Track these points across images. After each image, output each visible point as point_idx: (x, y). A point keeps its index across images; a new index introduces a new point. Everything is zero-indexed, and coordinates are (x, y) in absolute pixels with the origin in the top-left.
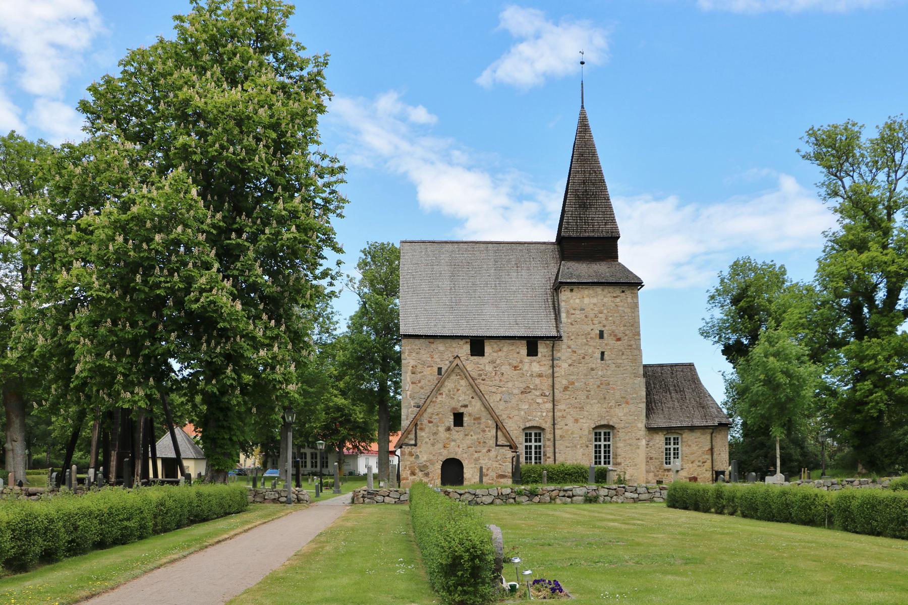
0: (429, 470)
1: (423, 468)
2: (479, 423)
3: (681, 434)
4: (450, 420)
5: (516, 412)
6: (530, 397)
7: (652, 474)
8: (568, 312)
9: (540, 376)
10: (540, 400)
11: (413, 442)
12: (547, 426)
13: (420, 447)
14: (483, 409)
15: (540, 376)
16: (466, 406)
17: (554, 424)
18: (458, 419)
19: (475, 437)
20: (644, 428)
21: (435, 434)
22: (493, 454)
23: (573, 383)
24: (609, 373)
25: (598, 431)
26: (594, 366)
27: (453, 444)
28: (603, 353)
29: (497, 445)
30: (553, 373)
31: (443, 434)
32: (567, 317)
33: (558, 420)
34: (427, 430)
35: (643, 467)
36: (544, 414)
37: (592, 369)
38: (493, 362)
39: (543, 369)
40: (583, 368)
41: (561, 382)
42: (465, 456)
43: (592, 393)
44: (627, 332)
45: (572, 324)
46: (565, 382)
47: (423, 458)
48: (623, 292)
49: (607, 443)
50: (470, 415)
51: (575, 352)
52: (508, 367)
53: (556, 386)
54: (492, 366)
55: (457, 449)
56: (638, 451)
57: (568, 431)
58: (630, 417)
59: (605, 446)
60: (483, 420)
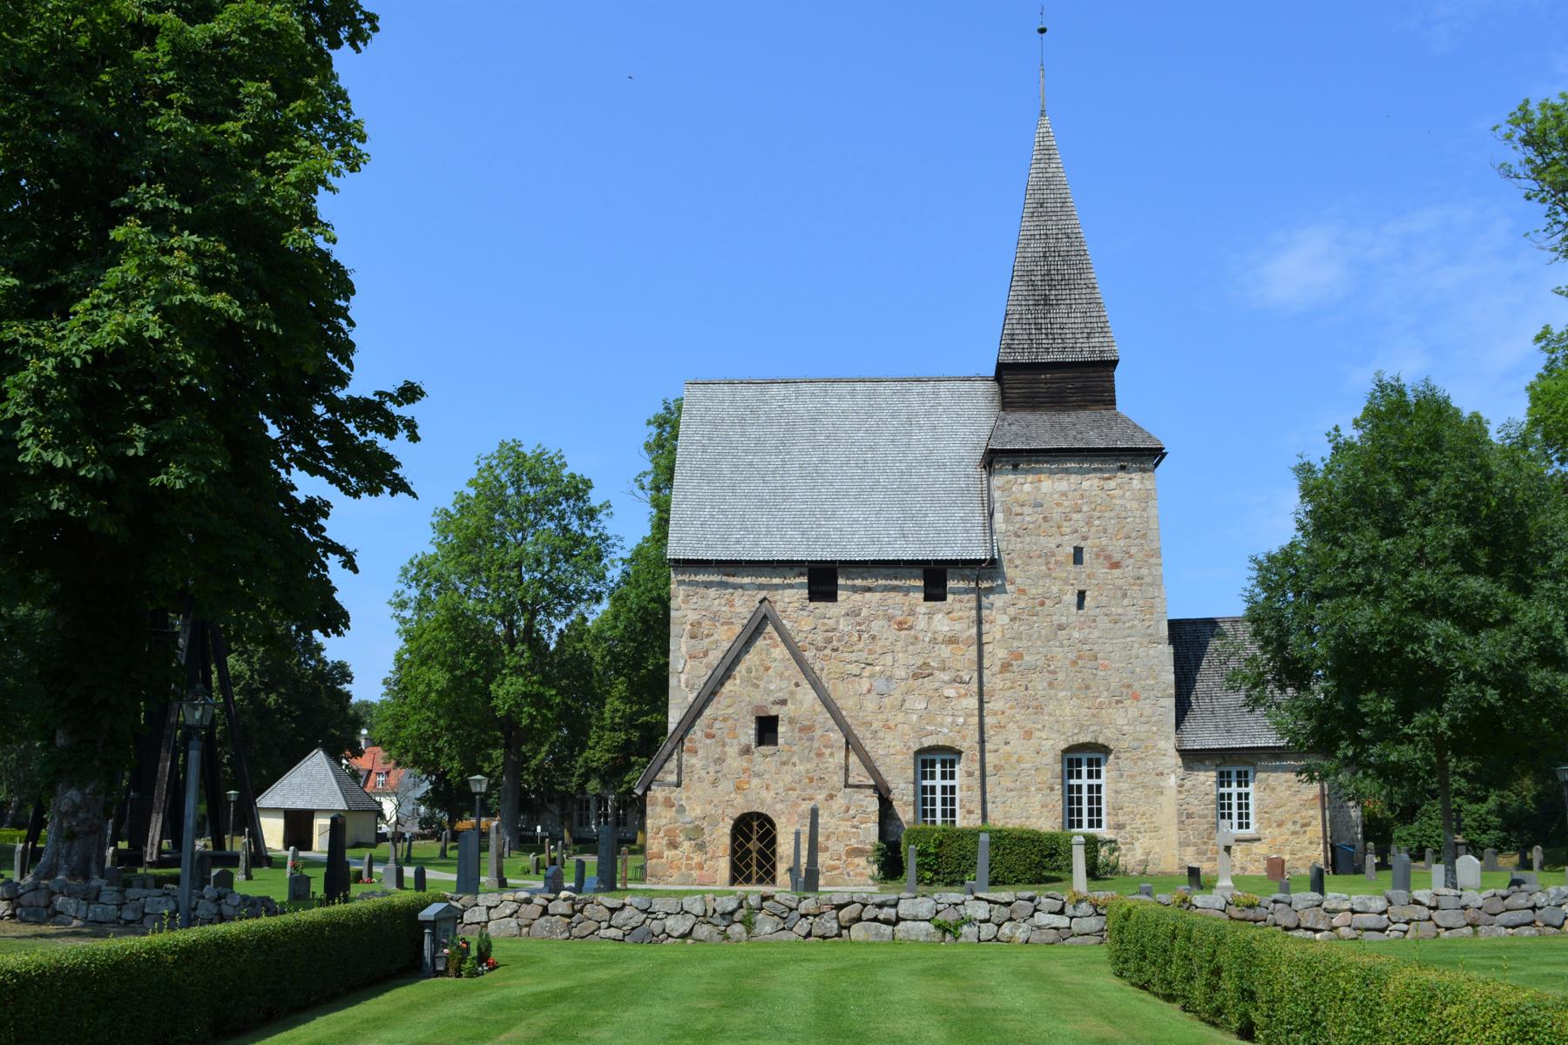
0: (706, 837)
1: (695, 834)
2: (812, 739)
4: (749, 733)
5: (900, 717)
7: (1191, 850)
8: (1008, 512)
9: (952, 641)
10: (950, 692)
12: (968, 744)
13: (687, 787)
14: (819, 707)
15: (952, 641)
16: (783, 702)
17: (982, 742)
18: (767, 729)
20: (1173, 752)
21: (720, 760)
22: (840, 802)
23: (1021, 656)
24: (1096, 634)
25: (1075, 756)
26: (1064, 620)
27: (755, 781)
28: (1081, 595)
30: (980, 634)
31: (735, 762)
32: (1007, 521)
33: (989, 732)
34: (701, 753)
35: (1172, 834)
36: (961, 720)
37: (1061, 627)
38: (853, 613)
39: (957, 627)
41: (996, 654)
42: (778, 807)
43: (1061, 676)
44: (1133, 550)
46: (1001, 653)
47: (695, 811)
48: (1123, 468)
49: (1094, 782)
50: (791, 721)
51: (1023, 592)
53: (986, 663)
54: (852, 620)
55: (764, 793)
56: (1160, 799)
57: (1009, 755)
58: (1142, 723)
59: (1090, 787)
60: (818, 733)
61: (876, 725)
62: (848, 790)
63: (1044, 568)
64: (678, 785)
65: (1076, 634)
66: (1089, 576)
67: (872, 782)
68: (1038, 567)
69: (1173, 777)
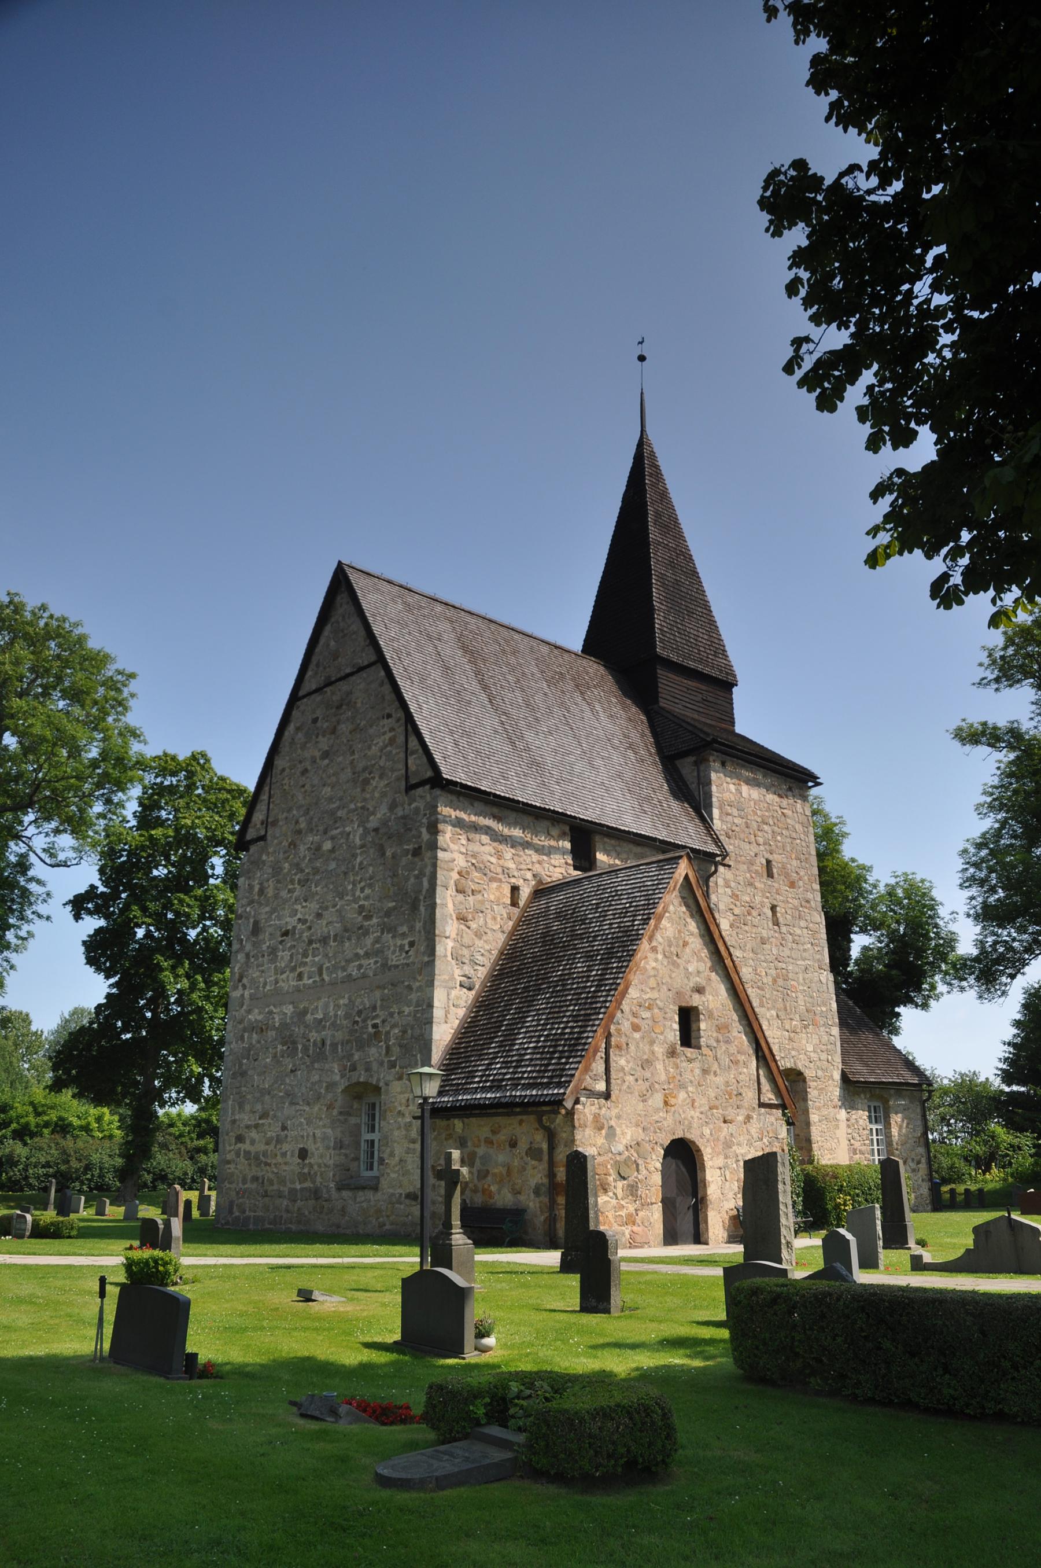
11: (601, 1086)
22: (754, 1128)
29: (762, 1105)
31: (661, 1069)
56: (837, 1131)
62: (763, 1110)
64: (607, 1095)
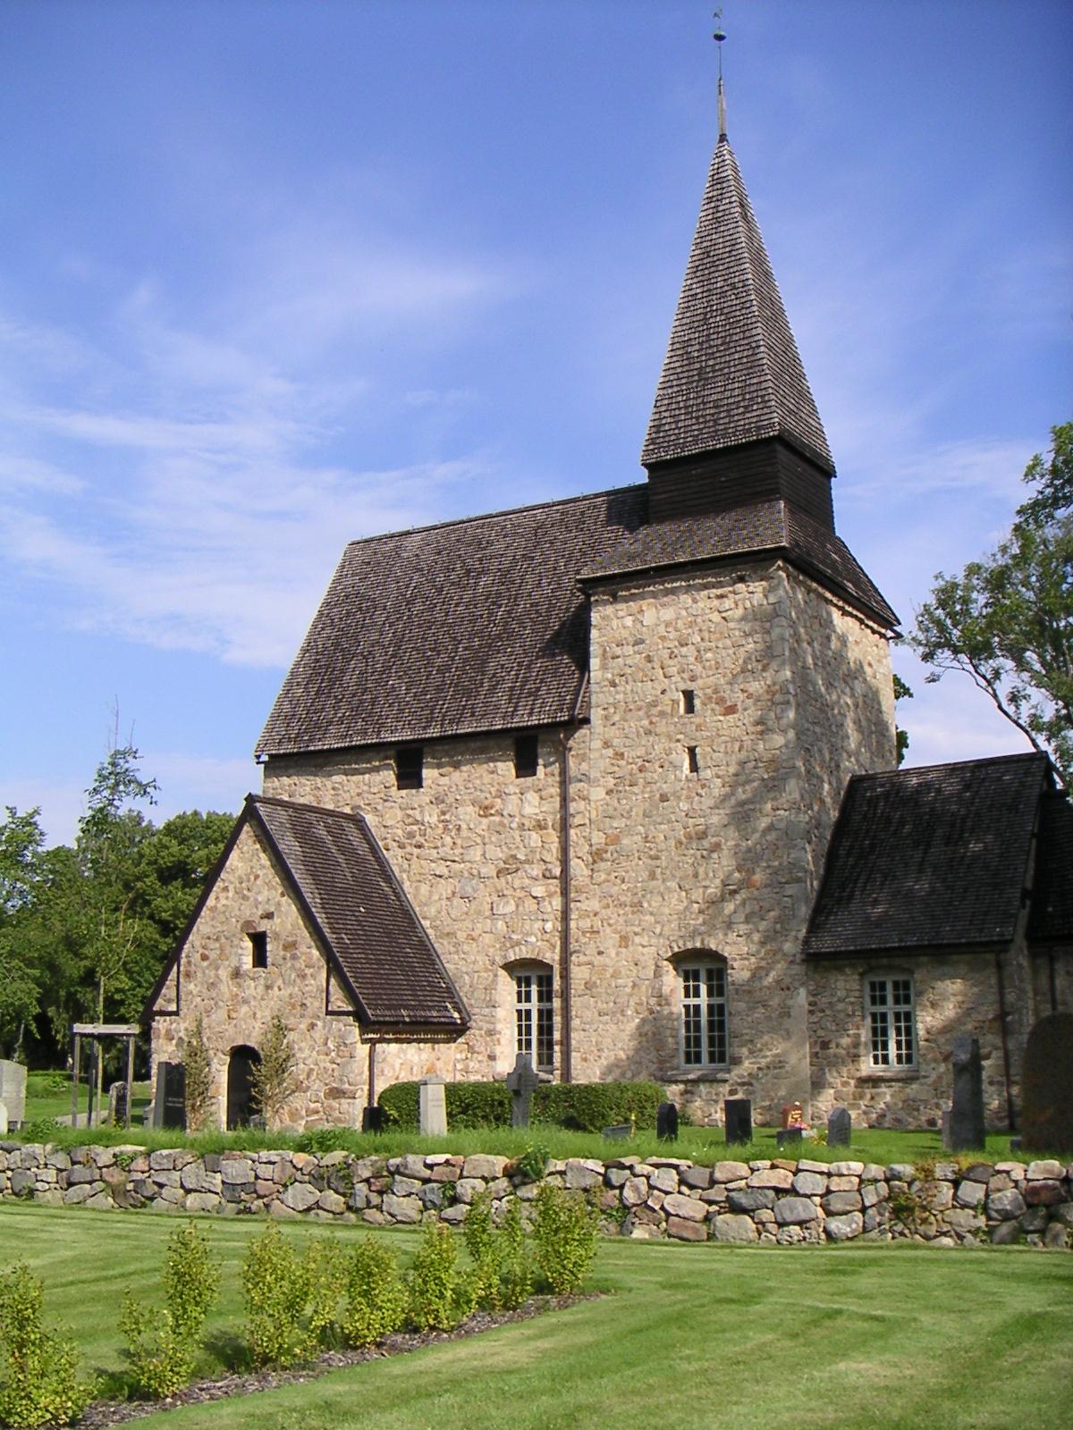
2: (294, 957)
3: (911, 972)
6: (517, 884)
15: (540, 826)
16: (269, 916)
19: (285, 993)
23: (615, 840)
27: (244, 1009)
29: (328, 1013)
32: (604, 667)
37: (664, 798)
40: (637, 799)
45: (614, 685)
50: (277, 936)
52: (470, 809)
57: (604, 967)
60: (303, 949)
61: (461, 936)
62: (329, 1017)
63: (646, 722)
65: (684, 806)
66: (699, 728)
67: (350, 1009)
68: (638, 723)
69: (802, 991)
